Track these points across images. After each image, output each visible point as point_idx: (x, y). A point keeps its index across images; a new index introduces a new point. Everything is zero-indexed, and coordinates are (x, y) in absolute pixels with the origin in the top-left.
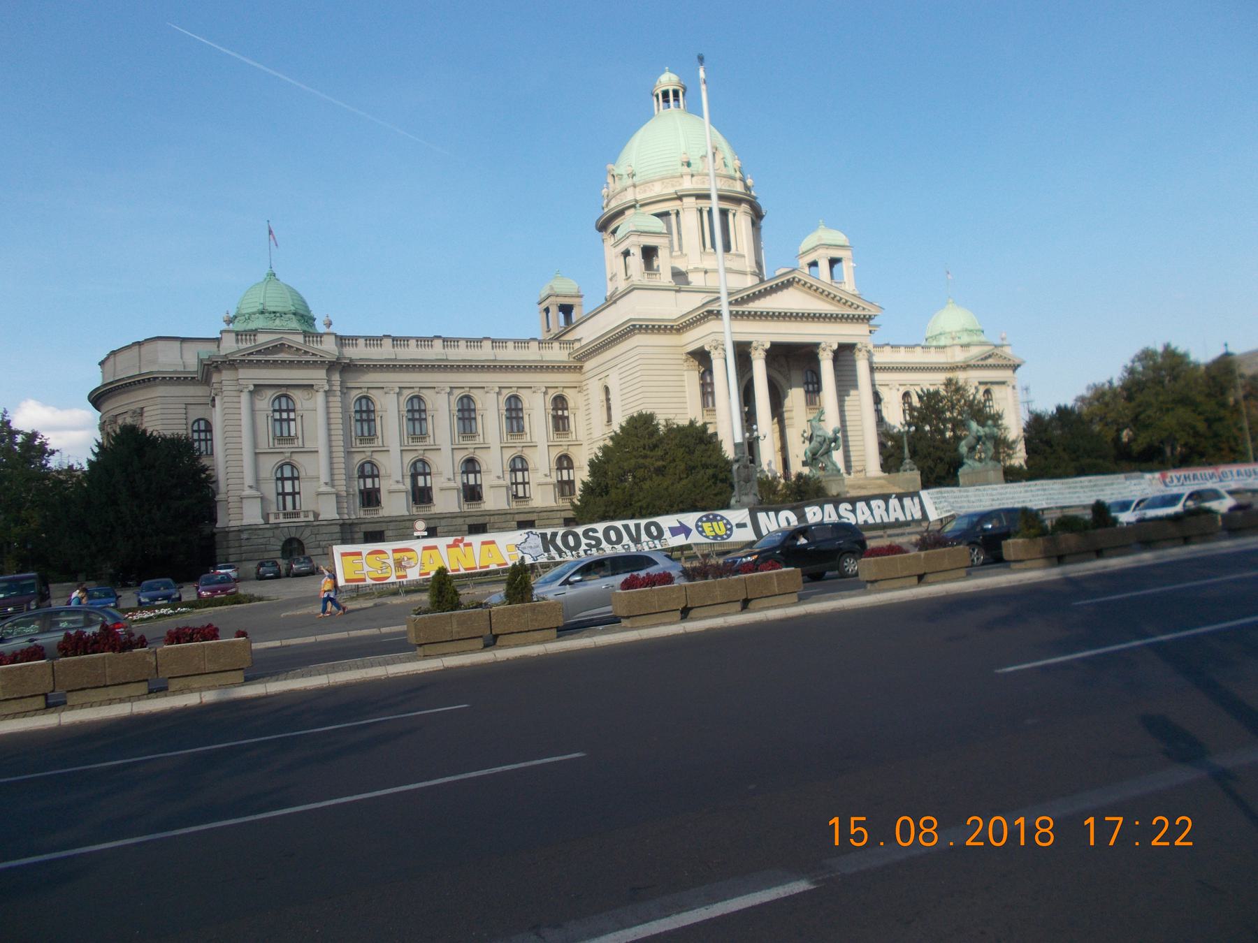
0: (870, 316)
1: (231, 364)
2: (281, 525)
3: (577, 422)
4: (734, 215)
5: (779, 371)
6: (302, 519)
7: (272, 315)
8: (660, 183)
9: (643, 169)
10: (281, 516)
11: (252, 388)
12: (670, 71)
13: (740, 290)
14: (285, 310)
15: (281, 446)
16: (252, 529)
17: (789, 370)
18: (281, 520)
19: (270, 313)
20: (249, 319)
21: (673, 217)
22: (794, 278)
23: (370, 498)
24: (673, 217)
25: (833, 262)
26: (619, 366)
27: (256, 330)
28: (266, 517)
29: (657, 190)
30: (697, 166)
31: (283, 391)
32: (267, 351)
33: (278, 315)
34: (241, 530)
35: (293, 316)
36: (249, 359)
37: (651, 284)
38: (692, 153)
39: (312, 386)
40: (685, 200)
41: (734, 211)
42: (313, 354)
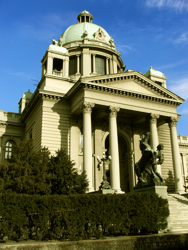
4: (109, 60)
17: (132, 132)
21: (78, 59)
22: (135, 76)
24: (78, 59)
26: (35, 122)
40: (84, 50)
41: (109, 59)
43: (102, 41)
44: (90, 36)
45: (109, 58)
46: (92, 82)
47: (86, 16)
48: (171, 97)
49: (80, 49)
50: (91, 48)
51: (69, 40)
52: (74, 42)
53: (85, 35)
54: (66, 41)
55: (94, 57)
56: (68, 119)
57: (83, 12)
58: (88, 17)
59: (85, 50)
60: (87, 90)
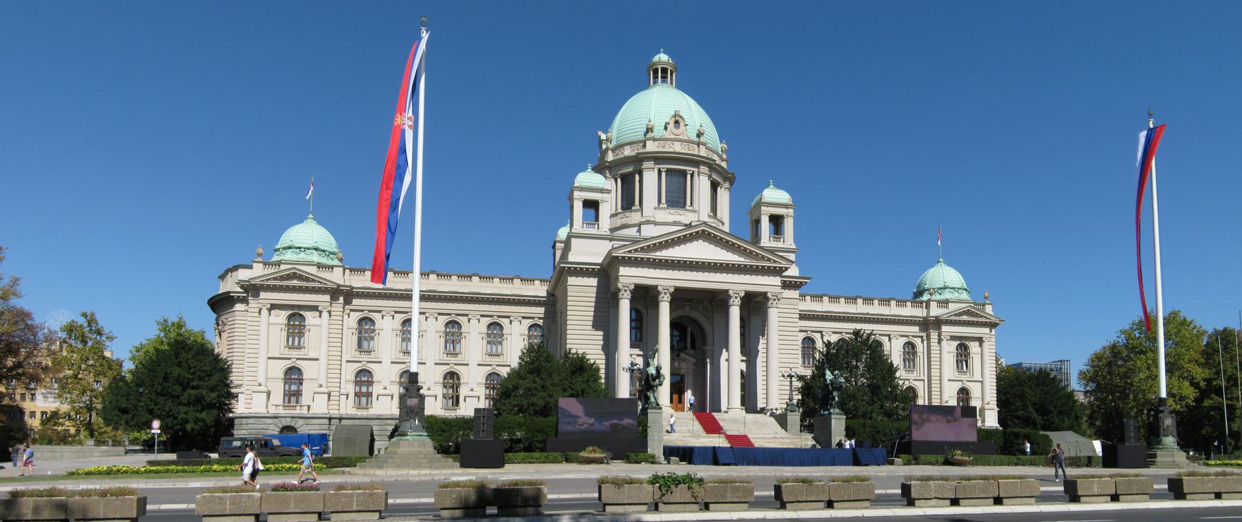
0: (781, 268)
5: (703, 315)
7: (298, 250)
12: (665, 53)
13: (653, 238)
14: (309, 246)
15: (290, 353)
19: (296, 248)
21: (637, 177)
24: (637, 177)
25: (777, 221)
30: (658, 132)
32: (282, 278)
33: (302, 249)
35: (314, 251)
37: (587, 232)
38: (659, 121)
39: (318, 306)
42: (319, 282)
43: (681, 137)
45: (693, 171)
46: (630, 251)
47: (662, 69)
48: (769, 260)
49: (638, 160)
50: (658, 158)
51: (621, 138)
52: (630, 144)
53: (649, 130)
54: (619, 139)
55: (663, 174)
57: (656, 59)
59: (646, 165)
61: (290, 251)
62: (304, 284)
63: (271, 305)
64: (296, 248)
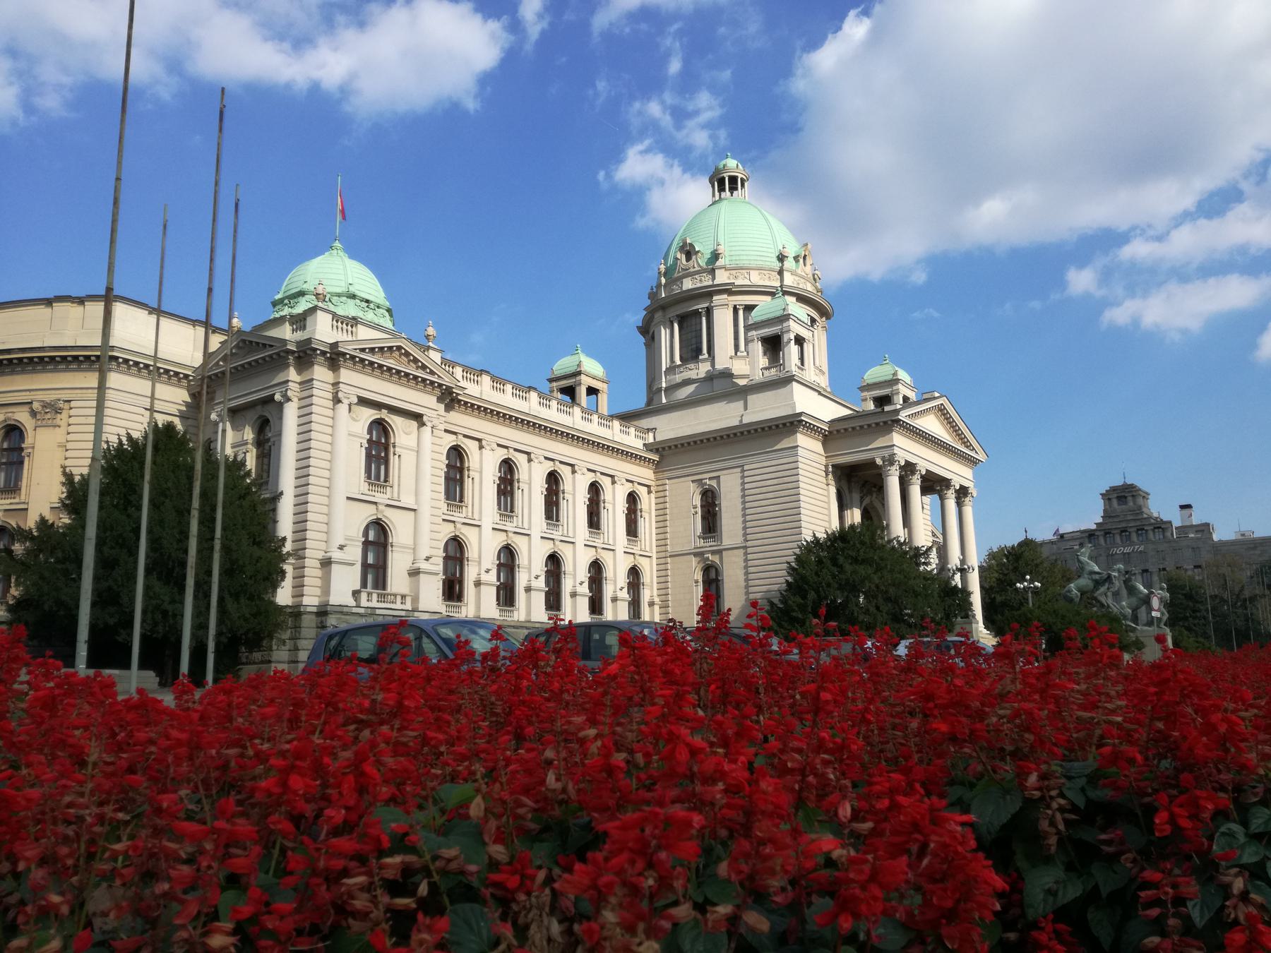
1: (335, 358)
2: (378, 612)
3: (647, 525)
6: (398, 606)
7: (364, 305)
8: (757, 272)
9: (733, 253)
10: (375, 597)
11: (355, 400)
16: (341, 610)
18: (374, 604)
20: (330, 301)
23: (453, 590)
27: (354, 318)
28: (356, 594)
29: (756, 279)
31: (384, 414)
33: (372, 306)
34: (323, 612)
35: (387, 314)
36: (362, 356)
42: (432, 373)
44: (789, 264)
51: (742, 258)
56: (824, 474)
58: (733, 180)
60: (898, 432)
61: (351, 302)
62: (412, 370)
63: (358, 397)
64: (362, 300)
